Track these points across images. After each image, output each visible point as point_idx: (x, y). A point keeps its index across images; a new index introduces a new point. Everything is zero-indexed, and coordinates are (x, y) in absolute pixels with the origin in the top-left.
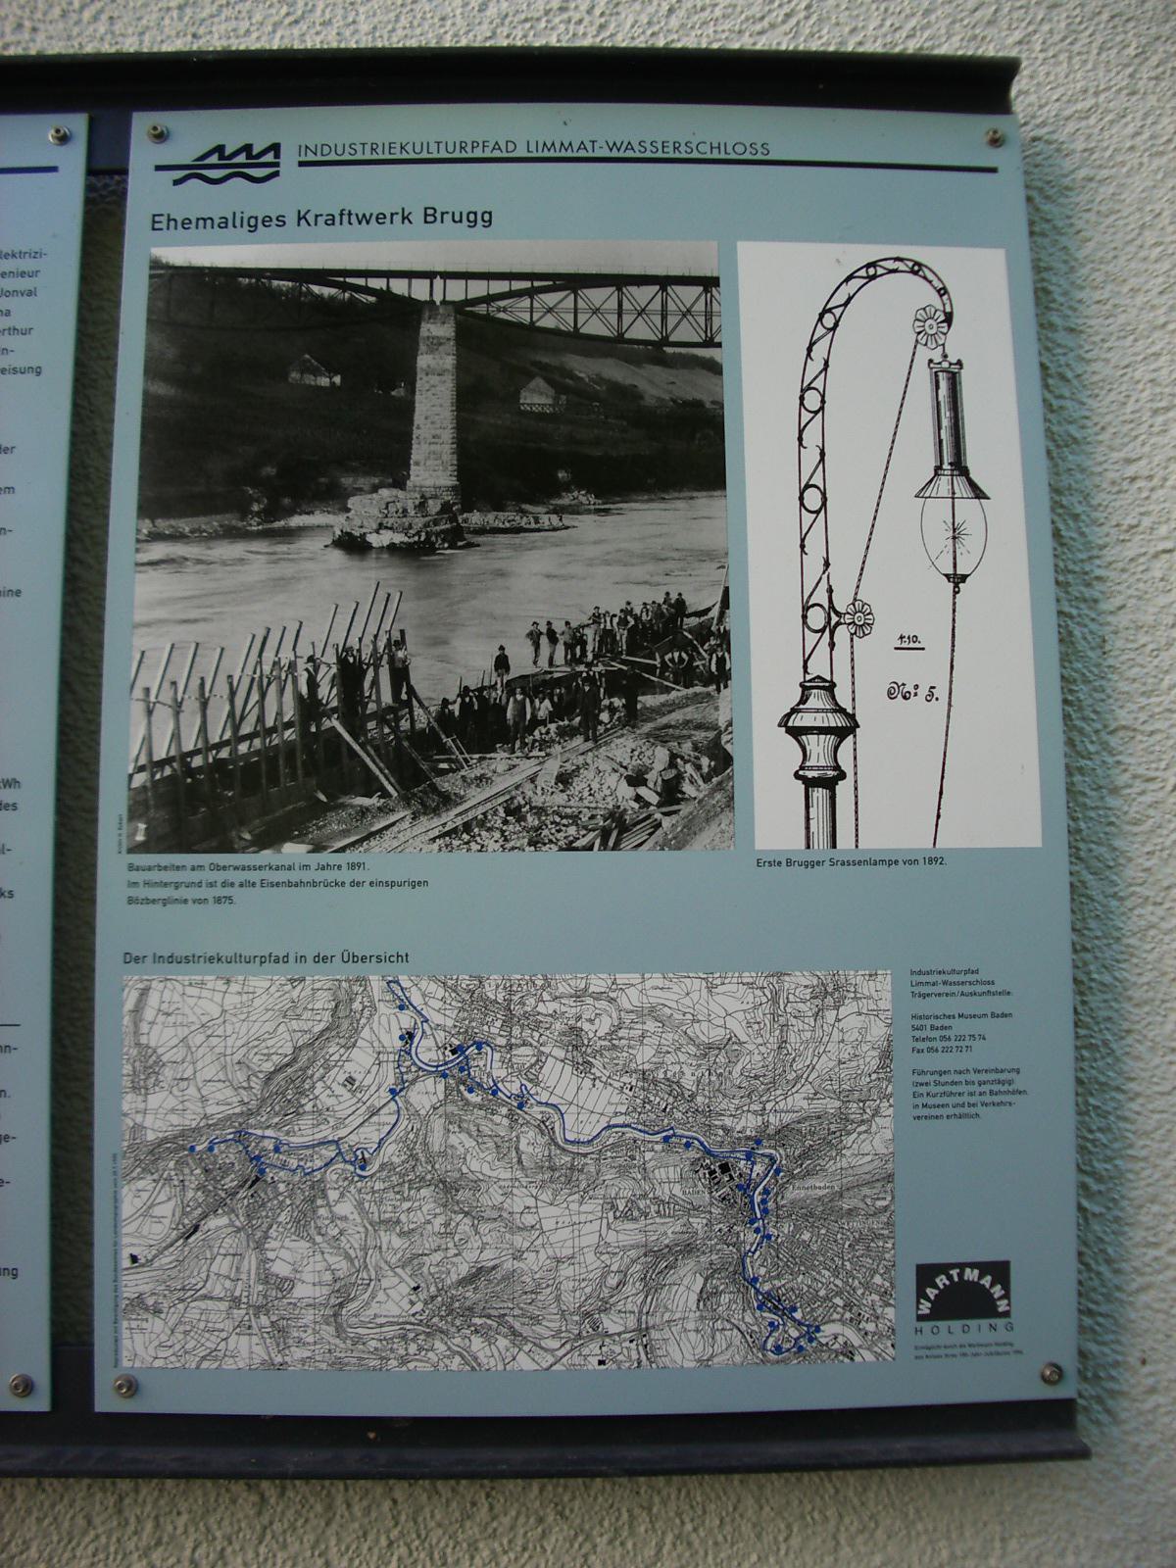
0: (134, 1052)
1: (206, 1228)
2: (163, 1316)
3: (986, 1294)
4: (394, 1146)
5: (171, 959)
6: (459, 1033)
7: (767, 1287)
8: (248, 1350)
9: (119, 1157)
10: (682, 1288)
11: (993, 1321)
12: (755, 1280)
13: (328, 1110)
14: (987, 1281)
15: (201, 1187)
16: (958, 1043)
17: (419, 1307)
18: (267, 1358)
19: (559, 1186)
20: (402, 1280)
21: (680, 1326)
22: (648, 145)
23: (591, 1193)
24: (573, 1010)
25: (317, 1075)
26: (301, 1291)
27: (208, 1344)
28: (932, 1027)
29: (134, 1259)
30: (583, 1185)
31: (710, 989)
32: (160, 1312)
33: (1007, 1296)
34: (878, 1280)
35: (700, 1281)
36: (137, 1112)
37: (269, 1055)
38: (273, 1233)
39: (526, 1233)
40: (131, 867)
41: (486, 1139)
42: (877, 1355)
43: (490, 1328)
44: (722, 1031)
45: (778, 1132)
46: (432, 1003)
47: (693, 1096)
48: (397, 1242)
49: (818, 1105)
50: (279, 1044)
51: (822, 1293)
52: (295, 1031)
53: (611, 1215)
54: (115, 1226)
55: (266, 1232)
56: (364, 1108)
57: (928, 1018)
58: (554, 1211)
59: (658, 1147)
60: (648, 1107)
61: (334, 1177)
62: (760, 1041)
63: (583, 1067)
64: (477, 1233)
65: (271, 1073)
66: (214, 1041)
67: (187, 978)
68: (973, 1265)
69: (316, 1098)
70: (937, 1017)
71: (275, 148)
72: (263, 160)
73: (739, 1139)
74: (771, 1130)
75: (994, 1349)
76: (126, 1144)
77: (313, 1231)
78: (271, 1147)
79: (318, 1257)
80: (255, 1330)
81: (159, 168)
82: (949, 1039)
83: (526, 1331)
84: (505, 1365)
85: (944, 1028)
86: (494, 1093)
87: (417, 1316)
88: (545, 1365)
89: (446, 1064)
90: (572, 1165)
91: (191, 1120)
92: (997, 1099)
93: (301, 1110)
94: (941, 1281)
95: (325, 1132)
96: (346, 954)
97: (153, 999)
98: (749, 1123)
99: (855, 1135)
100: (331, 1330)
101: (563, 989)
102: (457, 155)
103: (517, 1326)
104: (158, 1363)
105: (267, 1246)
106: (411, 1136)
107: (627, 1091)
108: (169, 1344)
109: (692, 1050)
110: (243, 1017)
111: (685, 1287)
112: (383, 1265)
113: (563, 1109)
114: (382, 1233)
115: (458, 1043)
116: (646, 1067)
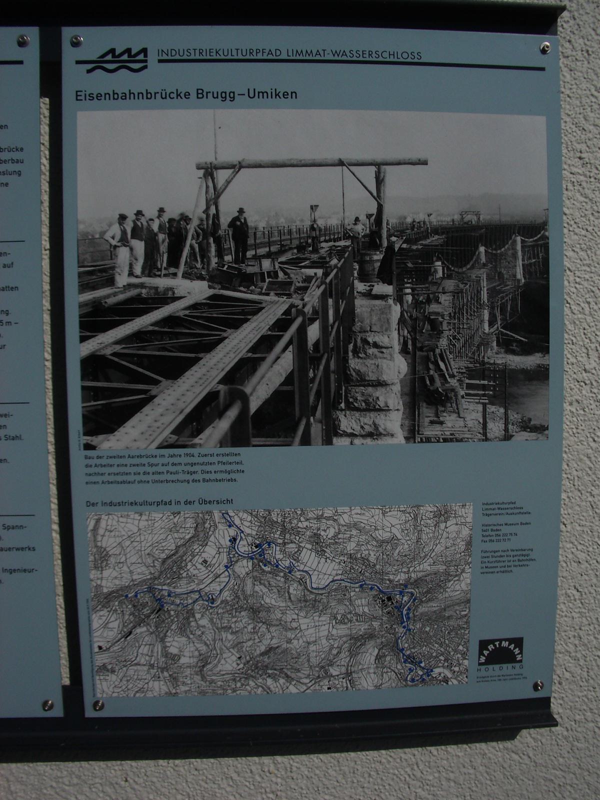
0: (95, 550)
1: (135, 633)
2: (116, 673)
3: (512, 652)
4: (227, 592)
5: (111, 504)
6: (259, 538)
7: (408, 652)
8: (159, 687)
9: (90, 601)
10: (368, 654)
11: (514, 665)
12: (403, 649)
13: (194, 576)
14: (512, 647)
15: (132, 614)
16: (504, 538)
17: (241, 666)
18: (168, 691)
19: (309, 609)
20: (233, 654)
21: (366, 671)
22: (354, 53)
23: (325, 612)
24: (316, 525)
25: (188, 559)
26: (183, 660)
27: (139, 685)
28: (492, 530)
29: (100, 648)
30: (321, 608)
31: (383, 514)
32: (115, 671)
33: (521, 653)
34: (461, 648)
35: (376, 651)
36: (98, 579)
37: (164, 550)
38: (169, 634)
39: (293, 631)
40: (86, 457)
41: (273, 588)
42: (459, 681)
43: (276, 674)
44: (389, 534)
45: (416, 581)
46: (245, 523)
47: (375, 565)
48: (230, 637)
49: (435, 568)
50: (168, 545)
51: (434, 654)
52: (176, 538)
53: (334, 622)
54: (90, 633)
55: (166, 634)
56: (212, 575)
57: (490, 525)
58: (306, 621)
59: (357, 590)
60: (352, 571)
61: (198, 608)
62: (408, 538)
63: (321, 553)
64: (269, 631)
65: (165, 559)
66: (135, 544)
67: (120, 513)
68: (506, 640)
69: (188, 570)
70: (494, 525)
71: (144, 51)
72: (137, 58)
73: (397, 585)
74: (412, 580)
75: (514, 677)
76: (93, 594)
77: (188, 633)
78: (166, 594)
79: (192, 645)
80: (162, 678)
81: (78, 62)
82: (500, 536)
83: (293, 675)
84: (283, 691)
85: (497, 530)
86: (277, 566)
87: (241, 670)
88: (302, 690)
89: (253, 552)
90: (315, 599)
91: (125, 582)
92: (521, 563)
93: (181, 576)
94: (491, 647)
95: (193, 586)
96: (201, 500)
97: (103, 524)
98: (401, 577)
99: (452, 582)
100: (199, 677)
101: (310, 515)
102: (248, 57)
103: (289, 673)
104: (115, 695)
105: (166, 640)
106: (236, 587)
107: (342, 564)
108: (120, 686)
109: (375, 543)
110: (150, 532)
111: (369, 654)
112: (223, 647)
113: (311, 573)
114: (223, 633)
115: (258, 542)
116: (352, 552)
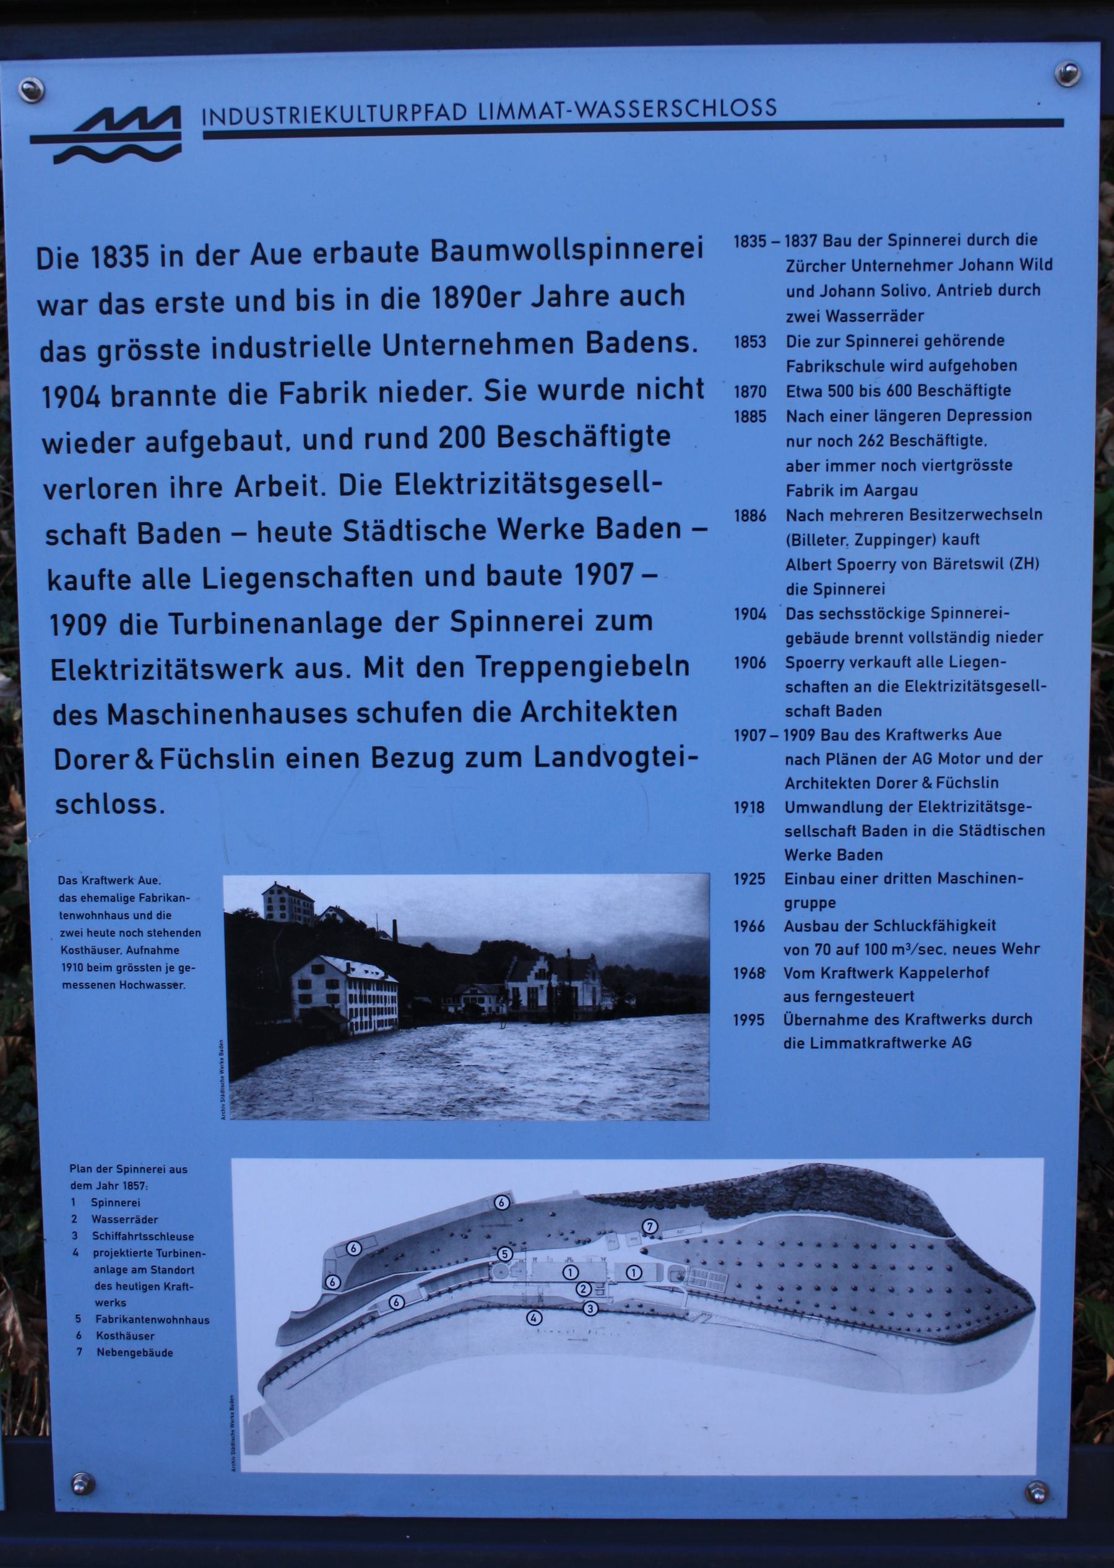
71: (174, 113)
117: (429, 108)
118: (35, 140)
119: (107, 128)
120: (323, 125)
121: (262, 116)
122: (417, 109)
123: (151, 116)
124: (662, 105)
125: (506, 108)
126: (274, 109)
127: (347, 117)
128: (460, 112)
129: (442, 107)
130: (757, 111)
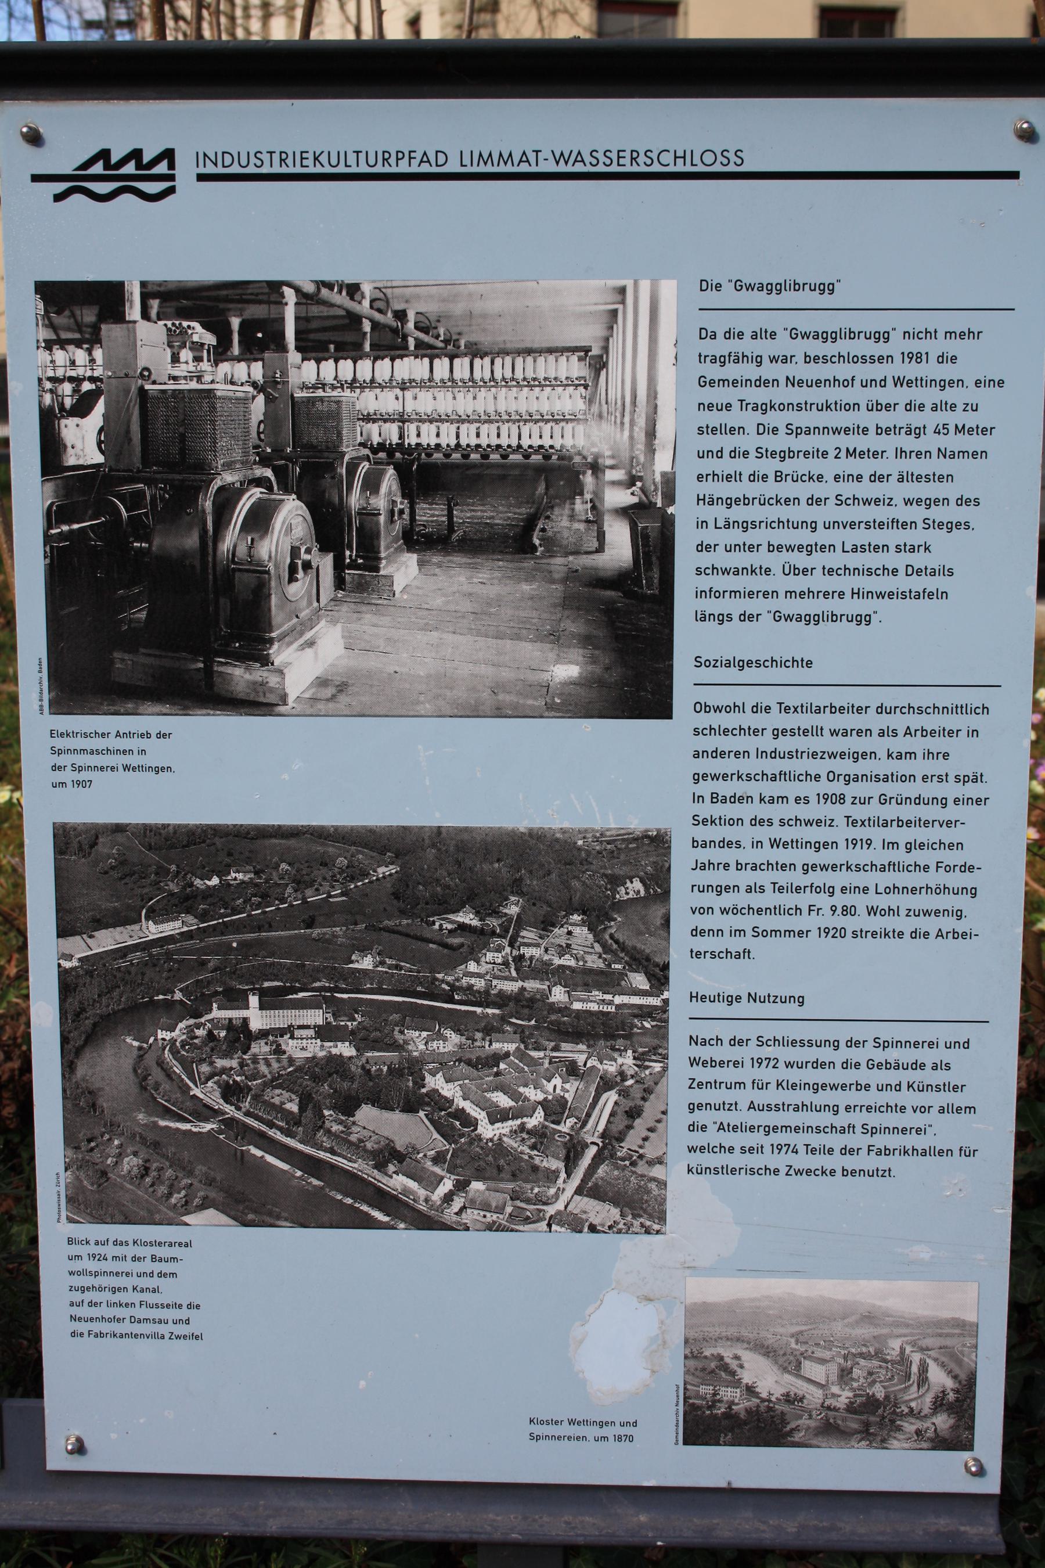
71: (168, 155)
102: (379, 169)
117: (413, 155)
118: (36, 178)
119: (105, 169)
120: (311, 170)
121: (253, 160)
122: (400, 155)
123: (146, 158)
124: (635, 155)
125: (485, 156)
126: (264, 152)
127: (334, 162)
128: (441, 161)
129: (425, 153)
130: (725, 161)
